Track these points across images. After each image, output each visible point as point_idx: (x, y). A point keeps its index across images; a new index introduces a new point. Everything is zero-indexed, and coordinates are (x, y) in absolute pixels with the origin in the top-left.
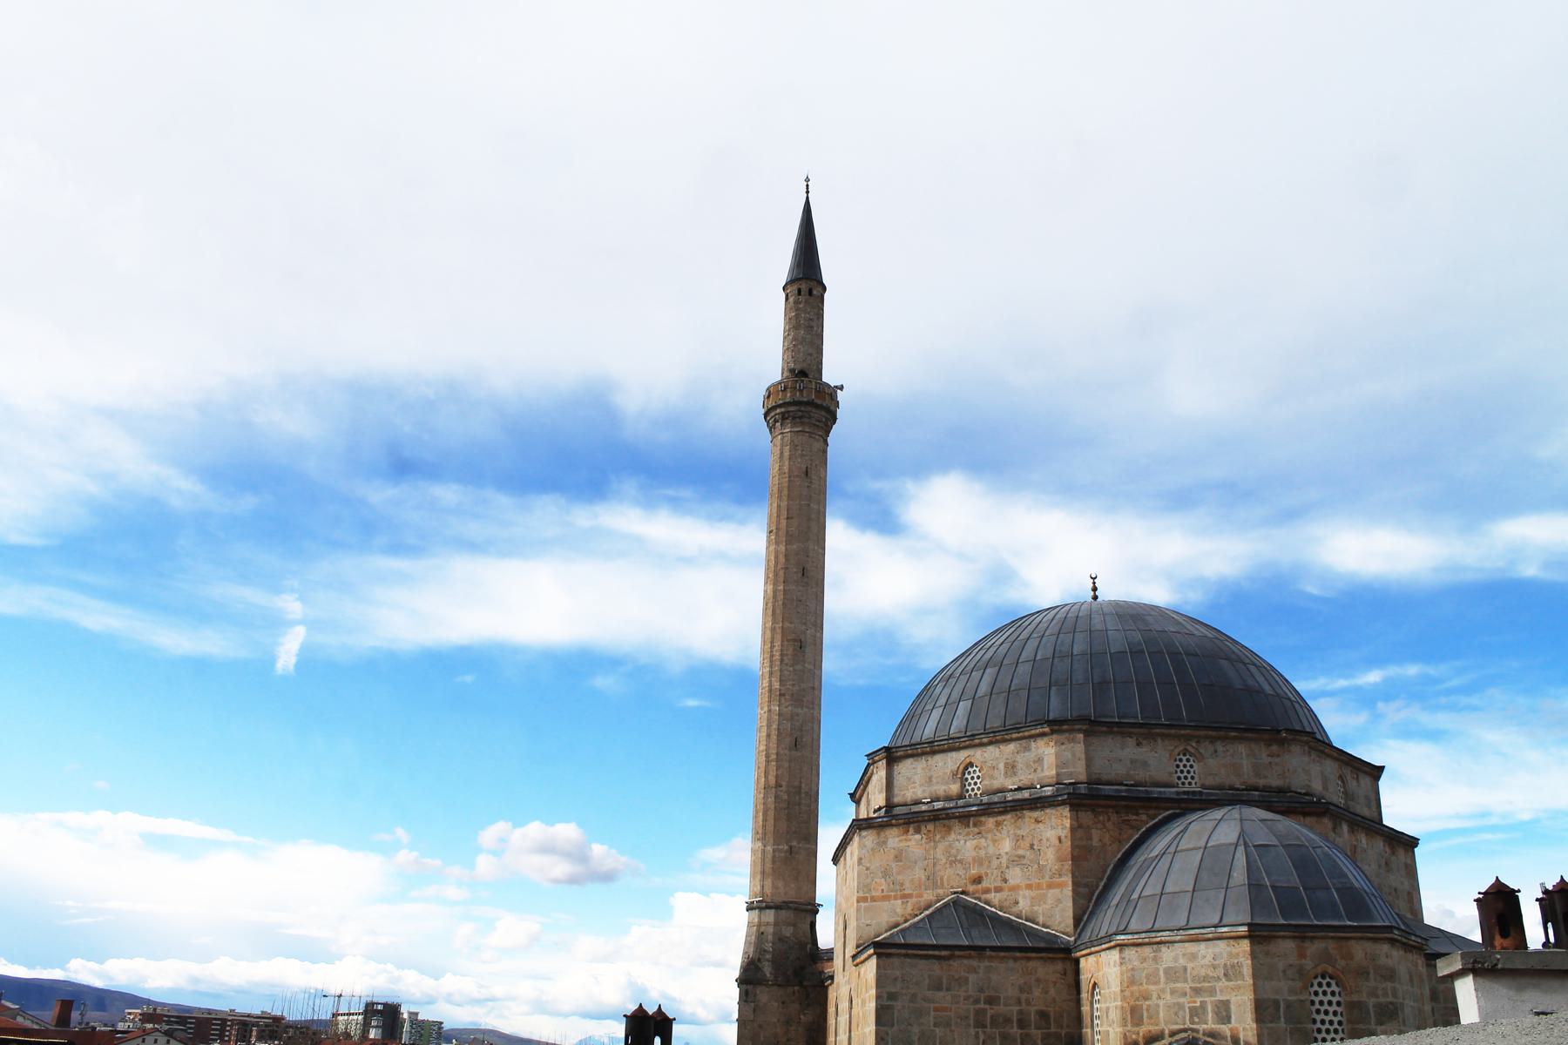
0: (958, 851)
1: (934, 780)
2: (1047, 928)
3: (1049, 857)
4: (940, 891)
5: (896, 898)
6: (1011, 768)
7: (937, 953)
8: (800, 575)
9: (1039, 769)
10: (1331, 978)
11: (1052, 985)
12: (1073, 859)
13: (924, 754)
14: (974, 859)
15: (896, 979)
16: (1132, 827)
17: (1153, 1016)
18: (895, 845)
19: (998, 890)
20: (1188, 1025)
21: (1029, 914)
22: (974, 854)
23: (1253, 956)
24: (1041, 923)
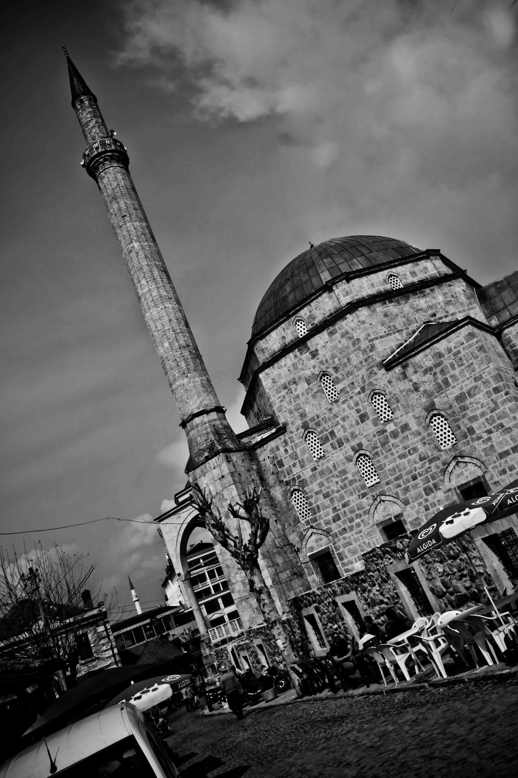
0: (418, 305)
1: (375, 285)
3: (463, 298)
4: (418, 324)
5: (394, 333)
6: (413, 274)
9: (427, 272)
14: (427, 307)
18: (381, 310)
19: (446, 317)
22: (426, 305)
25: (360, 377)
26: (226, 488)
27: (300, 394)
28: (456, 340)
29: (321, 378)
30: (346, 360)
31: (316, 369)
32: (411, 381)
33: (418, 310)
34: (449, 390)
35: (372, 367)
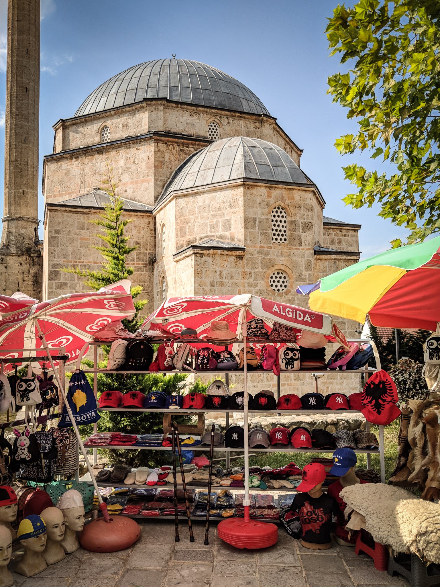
4: (88, 189)
7: (82, 210)
8: (25, 53)
9: (140, 126)
10: (282, 209)
11: (142, 229)
12: (155, 167)
13: (82, 122)
15: (60, 223)
16: (185, 153)
17: (191, 232)
20: (209, 233)
21: (132, 197)
23: (245, 195)
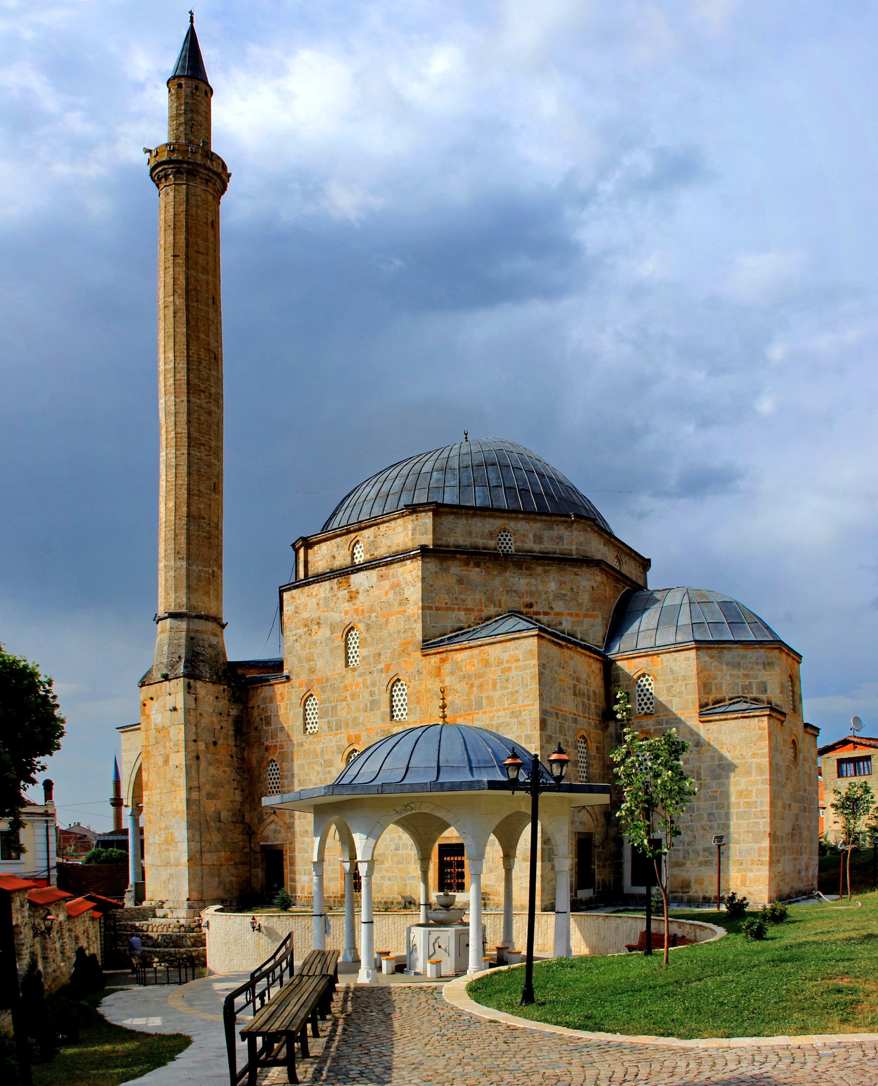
0: (514, 584)
2: (584, 641)
4: (500, 610)
5: (459, 609)
17: (719, 689)
19: (546, 614)
21: (570, 632)
22: (527, 588)
24: (579, 638)
25: (390, 651)
26: (174, 725)
27: (319, 642)
28: (512, 653)
29: (349, 631)
30: (383, 620)
31: (347, 617)
32: (442, 682)
33: (511, 591)
34: (478, 713)
35: (408, 643)
